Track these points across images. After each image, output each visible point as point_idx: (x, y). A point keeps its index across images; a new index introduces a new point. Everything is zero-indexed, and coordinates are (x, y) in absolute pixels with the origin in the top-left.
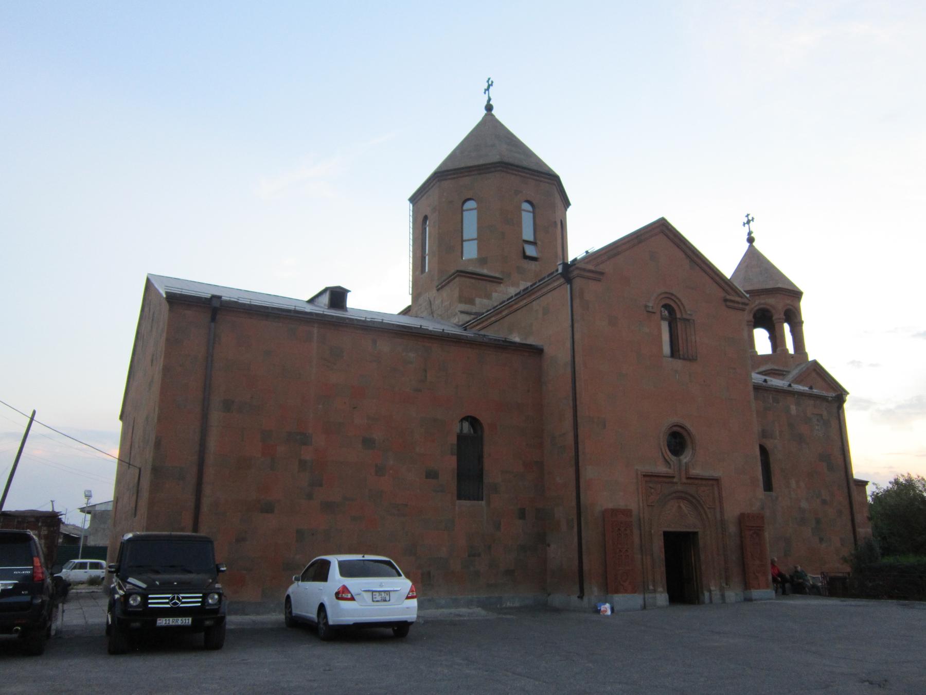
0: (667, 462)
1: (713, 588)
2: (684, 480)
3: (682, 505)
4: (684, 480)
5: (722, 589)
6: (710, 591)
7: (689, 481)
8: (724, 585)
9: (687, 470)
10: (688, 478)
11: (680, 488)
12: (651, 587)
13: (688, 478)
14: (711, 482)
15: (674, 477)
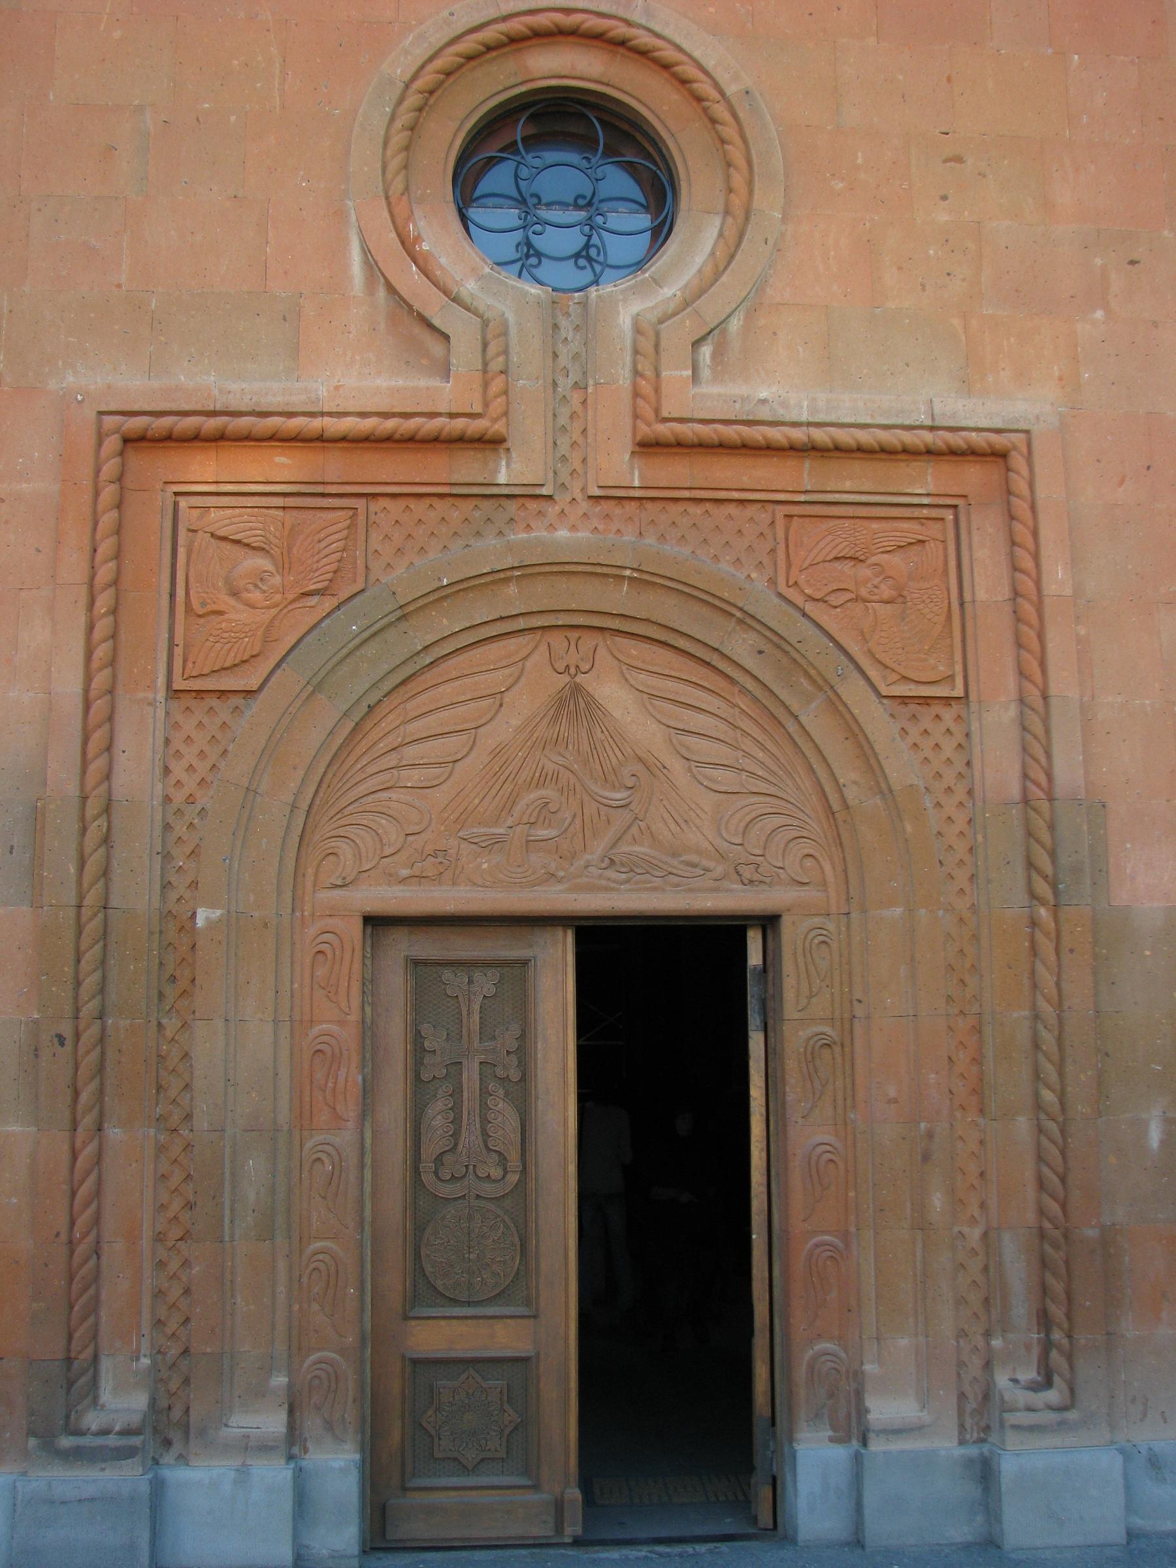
0: (414, 329)
1: (883, 1409)
2: (619, 466)
3: (612, 693)
4: (619, 466)
5: (981, 1414)
6: (854, 1428)
7: (676, 472)
8: (1012, 1380)
9: (646, 389)
10: (648, 447)
11: (566, 535)
12: (121, 1401)
13: (648, 447)
14: (924, 482)
15: (492, 443)
